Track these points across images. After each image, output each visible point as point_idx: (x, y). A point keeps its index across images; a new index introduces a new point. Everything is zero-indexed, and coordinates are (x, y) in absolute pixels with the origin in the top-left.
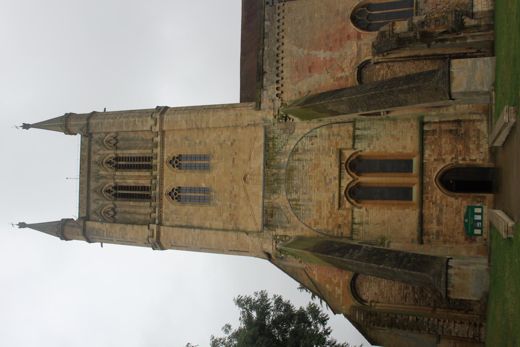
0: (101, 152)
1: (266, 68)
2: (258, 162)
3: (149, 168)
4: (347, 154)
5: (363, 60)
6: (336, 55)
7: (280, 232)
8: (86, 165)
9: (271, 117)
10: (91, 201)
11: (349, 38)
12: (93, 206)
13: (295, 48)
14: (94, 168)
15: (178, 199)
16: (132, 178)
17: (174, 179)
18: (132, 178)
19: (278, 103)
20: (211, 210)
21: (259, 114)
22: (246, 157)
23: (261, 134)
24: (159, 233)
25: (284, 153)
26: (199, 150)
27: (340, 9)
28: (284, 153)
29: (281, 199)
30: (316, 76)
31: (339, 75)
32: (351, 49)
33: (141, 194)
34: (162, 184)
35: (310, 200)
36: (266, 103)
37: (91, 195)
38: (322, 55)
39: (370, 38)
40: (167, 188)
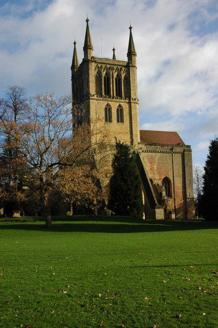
1: (152, 146)
3: (117, 95)
8: (117, 64)
9: (136, 148)
10: (103, 65)
12: (100, 65)
13: (158, 157)
14: (115, 67)
15: (106, 109)
16: (113, 87)
17: (114, 106)
18: (113, 87)
19: (140, 151)
21: (137, 143)
24: (92, 99)
26: (125, 120)
30: (149, 165)
31: (149, 173)
32: (157, 177)
36: (140, 146)
37: (105, 65)
38: (155, 166)
39: (160, 183)
40: (110, 103)
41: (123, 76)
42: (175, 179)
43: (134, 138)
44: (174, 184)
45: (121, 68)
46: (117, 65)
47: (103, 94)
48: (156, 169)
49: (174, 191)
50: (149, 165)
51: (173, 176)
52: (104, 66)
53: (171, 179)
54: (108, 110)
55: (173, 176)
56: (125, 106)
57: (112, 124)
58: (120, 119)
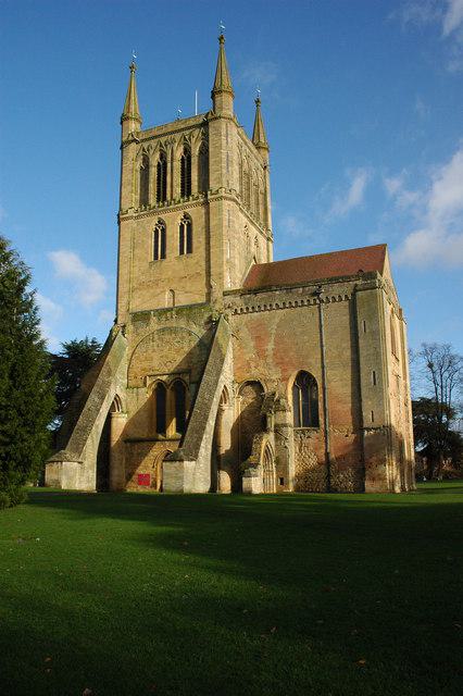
0: (193, 140)
2: (183, 300)
4: (187, 378)
5: (264, 385)
6: (270, 360)
7: (130, 328)
9: (217, 307)
11: (284, 370)
12: (146, 145)
13: (277, 320)
20: (146, 265)
21: (220, 295)
22: (188, 289)
23: (203, 300)
24: (127, 219)
25: (188, 324)
27: (310, 360)
28: (188, 324)
29: (154, 325)
33: (161, 196)
34: (165, 211)
35: (154, 351)
38: (270, 346)
40: (162, 216)
41: (195, 151)
42: (328, 373)
43: (213, 283)
44: (324, 389)
45: (190, 134)
46: (183, 129)
47: (152, 200)
48: (270, 352)
49: (325, 410)
50: (252, 344)
51: (323, 367)
52: (153, 143)
53: (316, 374)
54: (161, 233)
55: (323, 367)
56: (196, 213)
57: (165, 262)
58: (187, 246)
